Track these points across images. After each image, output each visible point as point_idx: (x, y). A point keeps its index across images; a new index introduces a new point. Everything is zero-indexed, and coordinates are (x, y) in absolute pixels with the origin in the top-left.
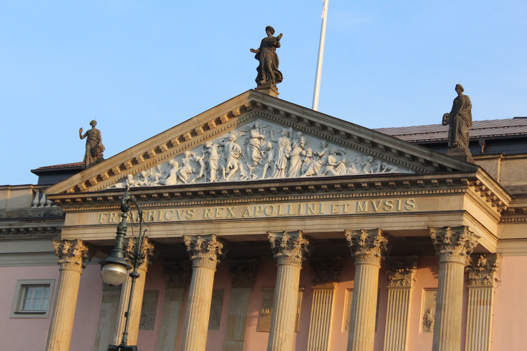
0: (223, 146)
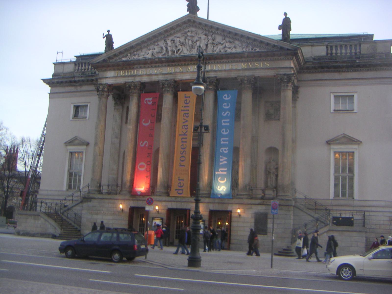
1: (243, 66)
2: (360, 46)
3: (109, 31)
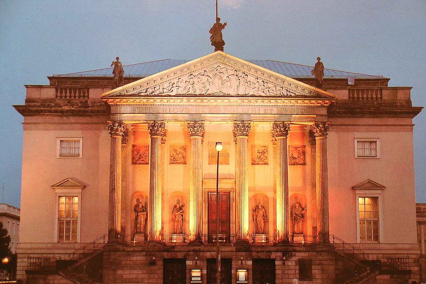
2: (381, 91)
3: (117, 58)
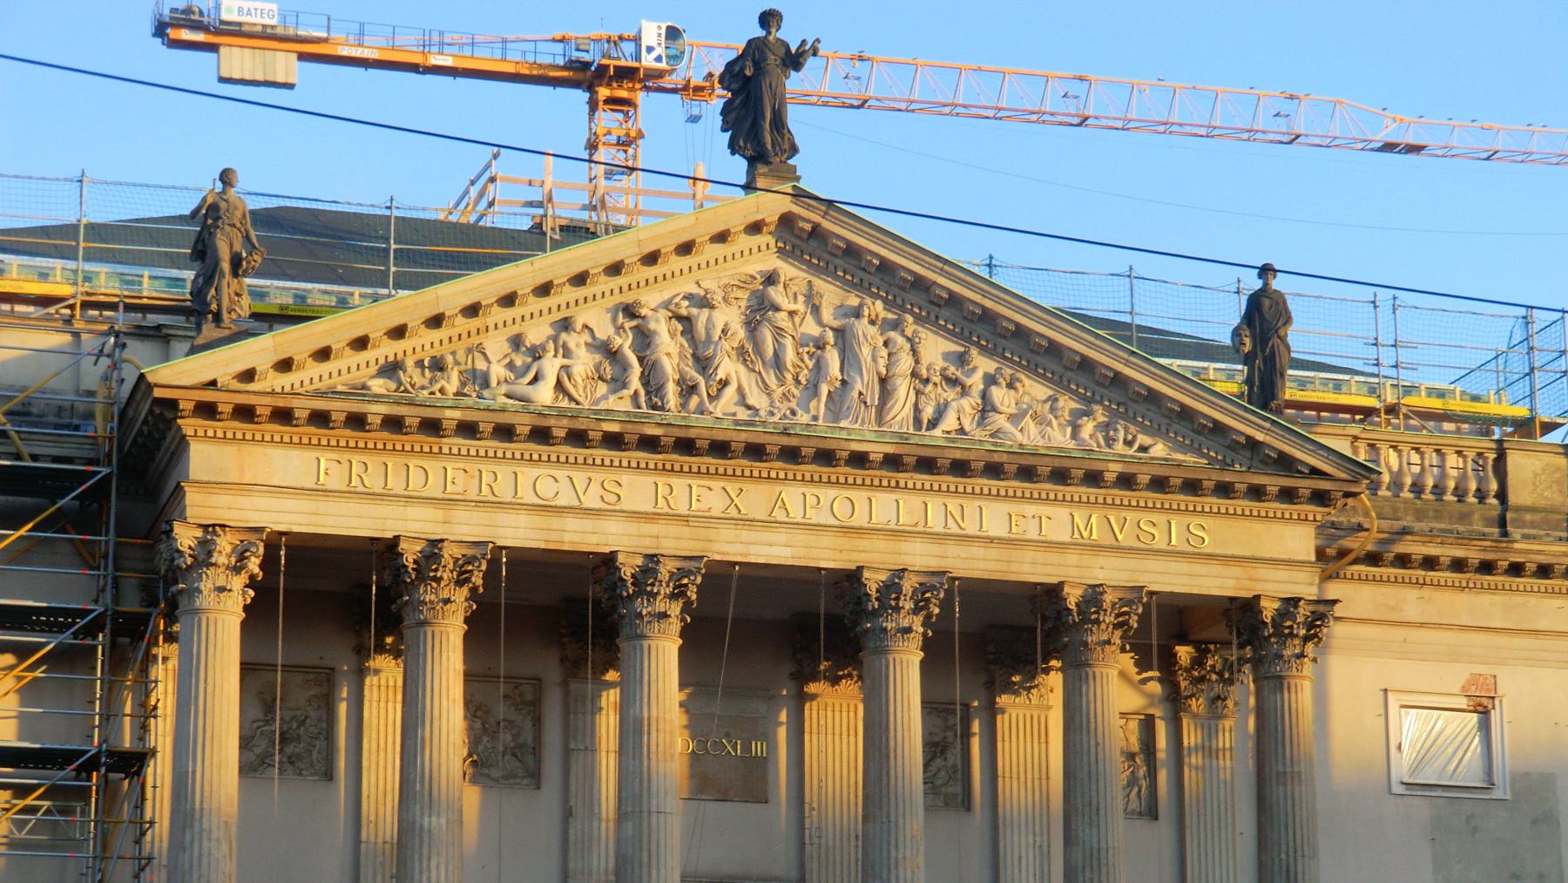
0: (686, 321)
1: (1093, 524)
